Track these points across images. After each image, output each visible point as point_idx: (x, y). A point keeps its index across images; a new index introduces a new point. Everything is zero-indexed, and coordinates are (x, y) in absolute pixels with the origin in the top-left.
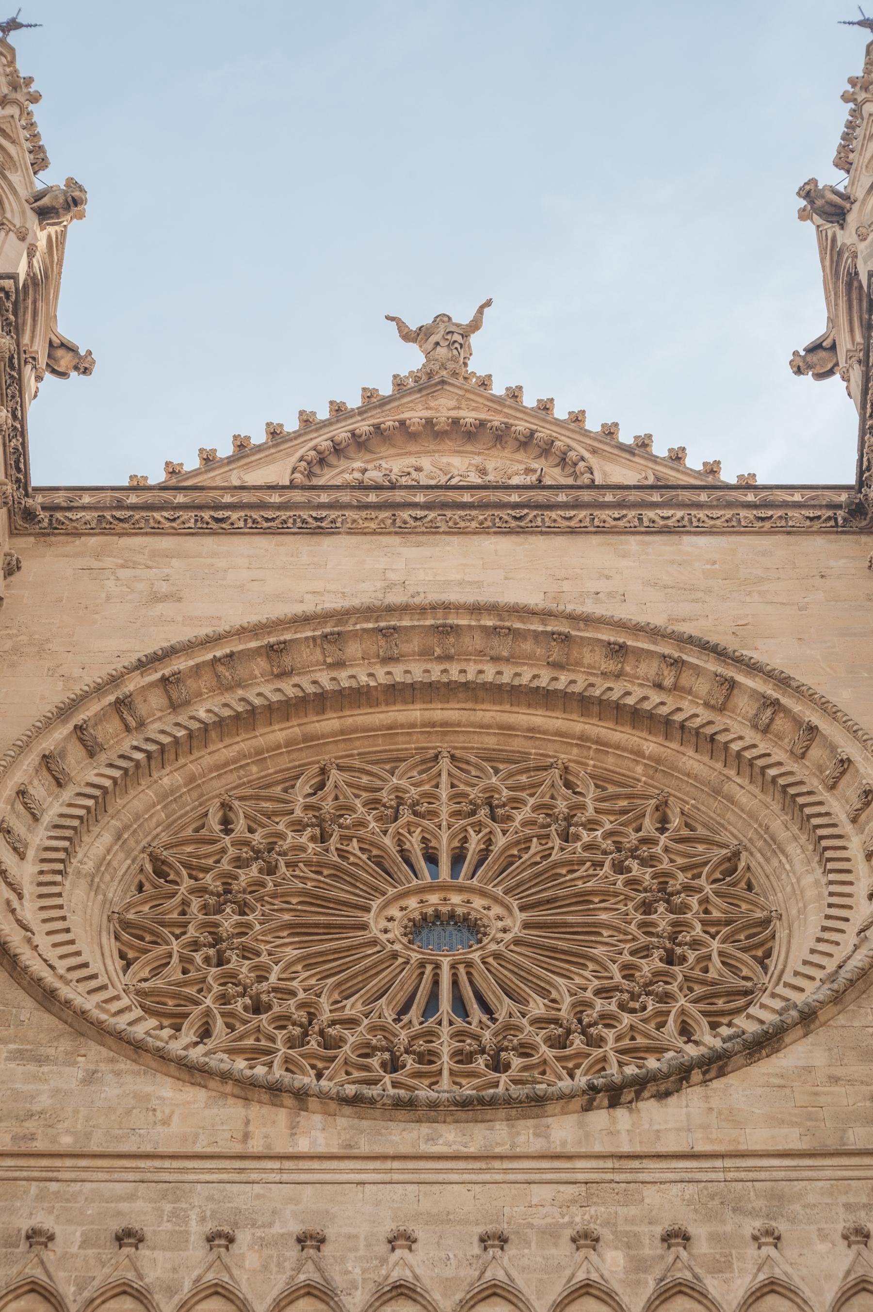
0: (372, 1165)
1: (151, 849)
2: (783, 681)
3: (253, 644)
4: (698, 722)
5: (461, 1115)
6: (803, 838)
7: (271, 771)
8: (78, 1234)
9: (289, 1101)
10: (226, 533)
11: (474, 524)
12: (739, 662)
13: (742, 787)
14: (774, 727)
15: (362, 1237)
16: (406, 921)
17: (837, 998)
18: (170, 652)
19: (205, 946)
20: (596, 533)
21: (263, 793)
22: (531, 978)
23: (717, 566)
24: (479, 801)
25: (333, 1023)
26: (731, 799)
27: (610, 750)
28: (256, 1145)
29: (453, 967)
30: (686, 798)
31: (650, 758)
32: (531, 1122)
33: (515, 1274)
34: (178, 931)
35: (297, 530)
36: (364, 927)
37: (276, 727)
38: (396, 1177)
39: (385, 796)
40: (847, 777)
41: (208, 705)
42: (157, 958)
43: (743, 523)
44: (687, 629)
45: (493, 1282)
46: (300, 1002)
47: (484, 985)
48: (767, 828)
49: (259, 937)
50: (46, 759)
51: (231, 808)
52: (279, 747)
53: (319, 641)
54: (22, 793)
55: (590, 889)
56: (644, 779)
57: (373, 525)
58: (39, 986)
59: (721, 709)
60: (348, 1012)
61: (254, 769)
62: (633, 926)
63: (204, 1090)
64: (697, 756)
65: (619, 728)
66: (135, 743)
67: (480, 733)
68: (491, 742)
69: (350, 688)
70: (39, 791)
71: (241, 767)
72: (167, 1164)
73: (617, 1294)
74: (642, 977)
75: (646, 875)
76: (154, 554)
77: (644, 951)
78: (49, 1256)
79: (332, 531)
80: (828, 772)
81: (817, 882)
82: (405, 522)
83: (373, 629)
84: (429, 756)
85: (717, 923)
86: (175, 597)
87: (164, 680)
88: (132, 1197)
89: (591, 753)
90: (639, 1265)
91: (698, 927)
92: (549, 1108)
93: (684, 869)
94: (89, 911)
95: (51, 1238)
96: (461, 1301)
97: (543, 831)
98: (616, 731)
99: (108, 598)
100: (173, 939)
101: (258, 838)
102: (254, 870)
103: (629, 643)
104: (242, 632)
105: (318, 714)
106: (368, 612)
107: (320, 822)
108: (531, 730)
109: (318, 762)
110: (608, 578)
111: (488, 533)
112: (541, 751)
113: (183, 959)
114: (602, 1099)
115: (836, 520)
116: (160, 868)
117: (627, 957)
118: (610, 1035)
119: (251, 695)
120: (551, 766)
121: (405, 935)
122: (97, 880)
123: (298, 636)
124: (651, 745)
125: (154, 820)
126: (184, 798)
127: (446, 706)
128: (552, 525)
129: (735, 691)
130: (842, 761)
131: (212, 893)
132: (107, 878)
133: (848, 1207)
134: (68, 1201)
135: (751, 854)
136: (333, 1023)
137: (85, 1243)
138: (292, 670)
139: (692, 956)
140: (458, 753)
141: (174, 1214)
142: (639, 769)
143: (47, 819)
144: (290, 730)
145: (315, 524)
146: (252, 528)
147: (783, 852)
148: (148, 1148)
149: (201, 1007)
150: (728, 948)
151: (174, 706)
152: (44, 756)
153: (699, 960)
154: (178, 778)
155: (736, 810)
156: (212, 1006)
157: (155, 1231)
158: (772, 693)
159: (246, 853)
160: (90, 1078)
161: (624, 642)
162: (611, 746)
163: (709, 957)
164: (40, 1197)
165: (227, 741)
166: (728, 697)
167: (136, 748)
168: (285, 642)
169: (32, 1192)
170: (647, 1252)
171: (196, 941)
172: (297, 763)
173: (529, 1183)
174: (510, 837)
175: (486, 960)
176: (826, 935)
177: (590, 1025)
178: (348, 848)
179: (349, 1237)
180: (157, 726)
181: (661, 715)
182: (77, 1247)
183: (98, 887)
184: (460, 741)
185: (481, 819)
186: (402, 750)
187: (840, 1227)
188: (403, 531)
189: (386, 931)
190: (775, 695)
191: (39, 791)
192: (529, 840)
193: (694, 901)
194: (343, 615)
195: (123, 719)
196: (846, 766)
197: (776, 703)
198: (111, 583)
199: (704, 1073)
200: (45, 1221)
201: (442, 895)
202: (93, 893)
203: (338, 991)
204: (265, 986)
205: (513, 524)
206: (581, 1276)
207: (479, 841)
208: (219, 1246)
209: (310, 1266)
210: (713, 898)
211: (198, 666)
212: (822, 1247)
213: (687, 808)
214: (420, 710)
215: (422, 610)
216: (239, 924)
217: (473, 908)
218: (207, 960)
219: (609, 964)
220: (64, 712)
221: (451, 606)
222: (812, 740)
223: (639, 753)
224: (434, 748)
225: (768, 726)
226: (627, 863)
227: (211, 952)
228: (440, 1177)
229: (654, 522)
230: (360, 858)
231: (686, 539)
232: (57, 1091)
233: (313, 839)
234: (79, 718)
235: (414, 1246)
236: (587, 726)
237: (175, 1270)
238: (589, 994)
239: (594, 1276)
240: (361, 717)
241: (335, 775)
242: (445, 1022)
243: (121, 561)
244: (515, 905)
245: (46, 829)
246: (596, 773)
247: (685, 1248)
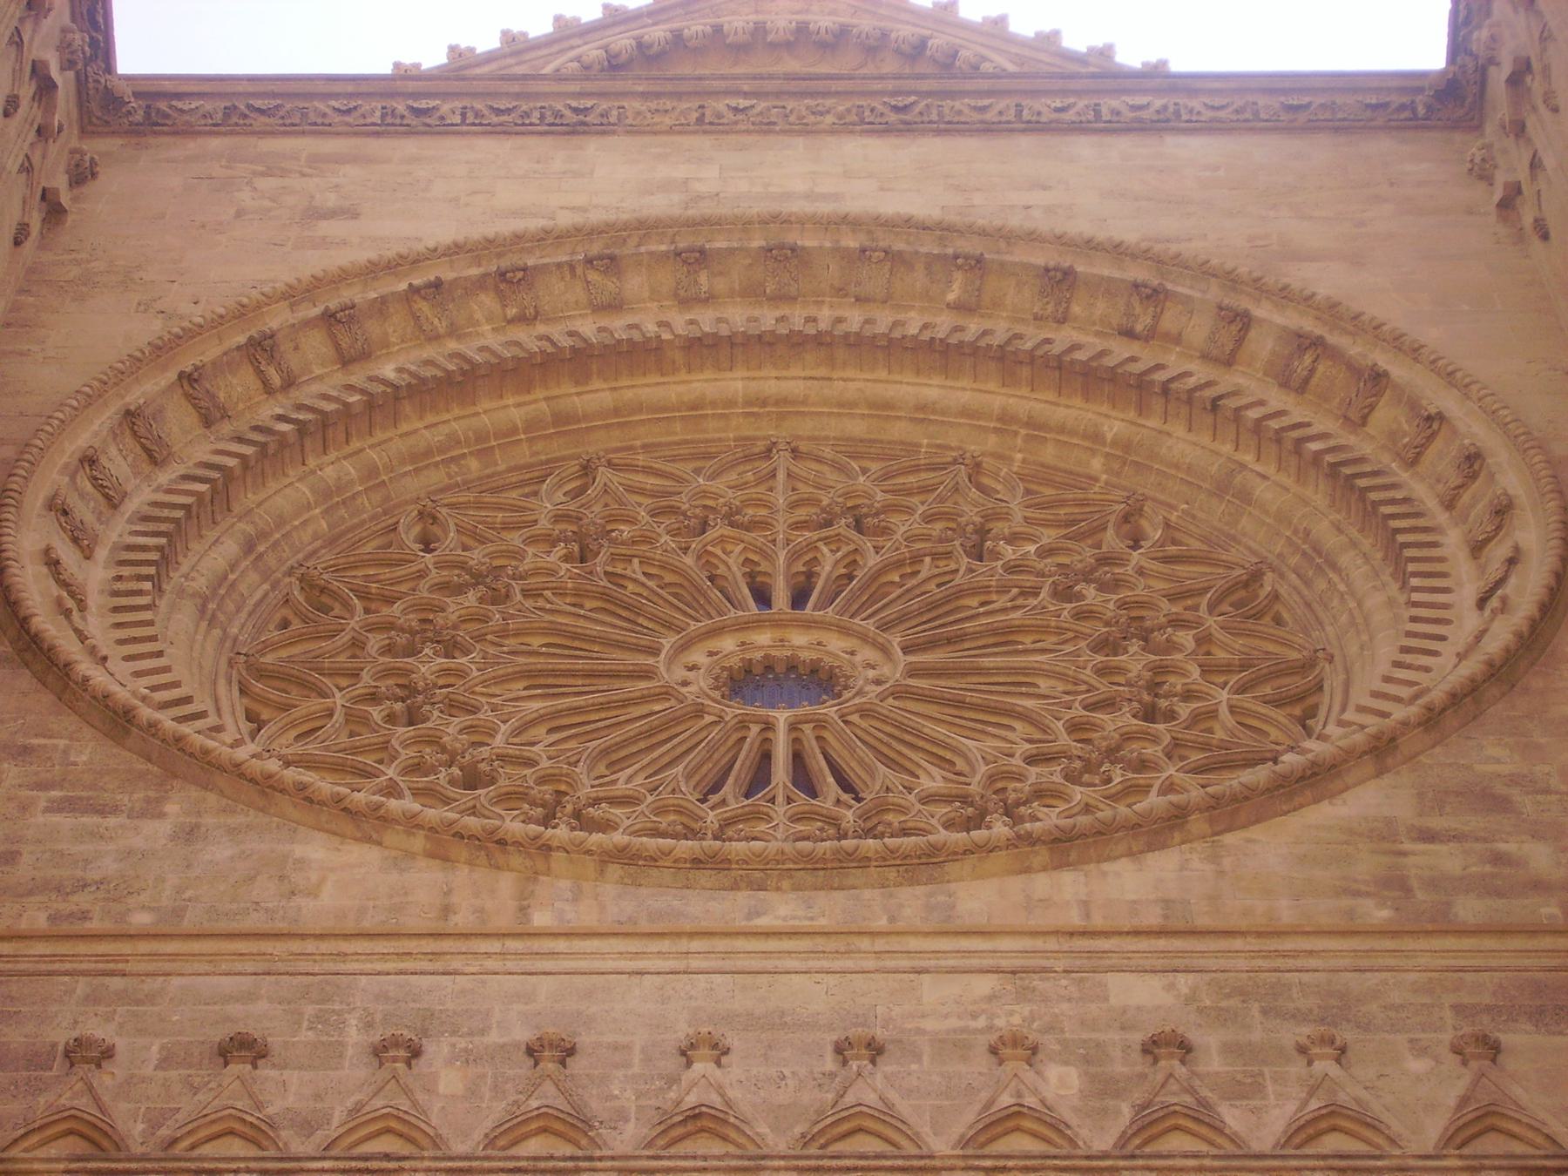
0: (655, 946)
1: (303, 570)
2: (1331, 311)
3: (474, 271)
4: (1191, 382)
5: (808, 878)
6: (1366, 543)
7: (502, 467)
8: (155, 1048)
10: (429, 131)
11: (829, 119)
12: (1258, 287)
13: (1264, 477)
14: (1314, 381)
15: (637, 1049)
16: (717, 670)
17: (1432, 720)
19: (388, 699)
20: (1023, 131)
21: (487, 498)
22: (921, 743)
23: (1221, 173)
24: (838, 510)
25: (596, 802)
26: (1245, 496)
27: (1048, 436)
28: (462, 919)
29: (793, 727)
30: (1174, 502)
31: (1114, 443)
32: (920, 890)
33: (893, 1096)
34: (344, 682)
35: (547, 128)
36: (647, 674)
37: (511, 401)
38: (695, 963)
39: (683, 502)
40: (1438, 444)
41: (402, 360)
42: (309, 718)
43: (1263, 116)
45: (858, 1109)
46: (542, 773)
47: (845, 753)
48: (1307, 533)
49: (477, 689)
50: (130, 415)
51: (434, 518)
52: (514, 430)
53: (579, 271)
54: (89, 460)
55: (1017, 623)
56: (1104, 477)
57: (668, 121)
58: (107, 706)
59: (1229, 362)
60: (621, 788)
61: (474, 464)
62: (1088, 671)
63: (375, 849)
64: (1192, 437)
65: (1063, 401)
66: (279, 411)
67: (839, 415)
69: (630, 340)
70: (118, 463)
71: (452, 459)
72: (310, 946)
73: (1068, 1127)
74: (1104, 738)
75: (1107, 604)
76: (315, 160)
77: (1108, 704)
78: (105, 1081)
79: (604, 128)
80: (1406, 440)
81: (1391, 602)
82: (719, 116)
83: (666, 255)
84: (756, 450)
85: (1227, 669)
87: (329, 317)
88: (250, 997)
89: (1019, 441)
90: (1103, 1088)
91: (1196, 672)
92: (952, 868)
93: (1173, 598)
94: (197, 646)
95: (108, 1053)
96: (803, 1136)
97: (941, 548)
98: (1058, 405)
99: (239, 214)
100: (335, 690)
101: (477, 556)
102: (471, 598)
103: (1080, 269)
104: (455, 250)
105: (577, 383)
107: (579, 537)
108: (921, 408)
109: (579, 457)
110: (1045, 188)
111: (851, 132)
112: (938, 442)
113: (350, 716)
115: (1414, 110)
116: (319, 594)
117: (1078, 711)
119: (469, 348)
120: (955, 462)
121: (716, 688)
122: (212, 606)
123: (546, 260)
124: (1115, 424)
125: (310, 530)
126: (359, 501)
127: (785, 373)
128: (956, 119)
129: (1252, 334)
130: (1429, 418)
131: (403, 630)
132: (230, 606)
133: (1458, 1009)
134: (138, 1002)
135: (1282, 576)
136: (596, 802)
137: (165, 1062)
138: (537, 313)
139: (1184, 710)
140: (803, 447)
141: (319, 1017)
142: (1096, 464)
143: (132, 506)
144: (533, 406)
145: (576, 118)
146: (474, 124)
147: (1334, 566)
148: (281, 926)
149: (378, 780)
150: (1246, 701)
152: (128, 413)
153: (1196, 718)
154: (350, 469)
155: (1256, 512)
156: (398, 779)
157: (286, 1043)
159: (455, 576)
160: (189, 834)
161: (1071, 267)
162: (1050, 430)
163: (1212, 714)
164: (92, 999)
165: (430, 418)
166: (1240, 342)
167: (281, 418)
168: (525, 269)
169: (79, 991)
170: (1119, 1068)
171: (374, 694)
172: (543, 458)
173: (919, 973)
174: (887, 555)
175: (850, 718)
176: (1408, 658)
177: (1018, 804)
178: (628, 572)
179: (616, 1047)
180: (315, 388)
181: (1130, 374)
182: (152, 1067)
183: (214, 616)
184: (806, 427)
185: (841, 530)
186: (713, 441)
187: (1447, 1037)
189: (685, 683)
190: (1318, 331)
191: (118, 463)
192: (916, 559)
193: (1186, 638)
195: (260, 373)
196: (1435, 426)
197: (1317, 343)
198: (245, 197)
199: (1211, 821)
201: (778, 634)
202: (204, 624)
203: (605, 762)
204: (485, 752)
205: (893, 117)
206: (1006, 1100)
207: (837, 562)
208: (395, 1060)
209: (548, 1087)
210: (1219, 635)
211: (383, 300)
212: (1418, 1065)
213: (1173, 517)
214: (742, 379)
215: (745, 224)
216: (446, 672)
217: (827, 652)
218: (391, 718)
219: (1048, 720)
220: (161, 350)
221: (793, 219)
222: (1379, 395)
223: (1096, 437)
224: (765, 438)
225: (1306, 381)
226: (1078, 588)
227: (398, 706)
228: (769, 964)
229: (1118, 113)
230: (643, 585)
231: (1170, 140)
232: (130, 852)
233: (567, 558)
235: (724, 1060)
236: (1011, 401)
237: (318, 1097)
238: (1017, 761)
239: (1030, 1101)
240: (647, 390)
241: (604, 475)
242: (780, 799)
243: (260, 168)
244: (895, 640)
245: (130, 521)
246: (1027, 471)
247: (1183, 1062)
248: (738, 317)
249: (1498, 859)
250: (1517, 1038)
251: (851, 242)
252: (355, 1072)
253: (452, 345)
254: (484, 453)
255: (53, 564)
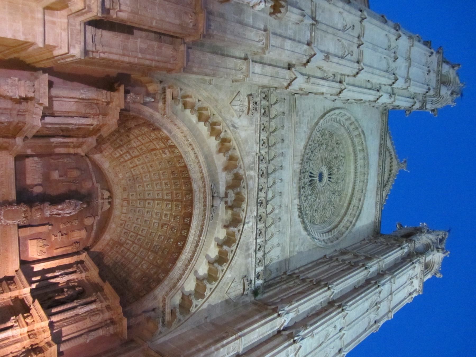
3: (364, 147)
9: (301, 162)
18: (364, 135)
26: (337, 217)
44: (362, 211)
54: (345, 115)
68: (347, 181)
86: (371, 133)
87: (360, 134)
88: (288, 140)
90: (276, 215)
104: (366, 145)
106: (368, 164)
114: (299, 207)
118: (306, 203)
124: (346, 205)
133: (282, 243)
137: (282, 135)
142: (342, 203)
143: (341, 118)
151: (356, 135)
158: (353, 223)
160: (305, 132)
188: (379, 166)
191: (345, 117)
194: (368, 159)
200: (285, 128)
212: (277, 240)
220: (356, 120)
223: (344, 203)
234: (355, 122)
248: (359, 170)
249: (297, 245)
250: (279, 249)
251: (365, 181)
252: (281, 151)
253: (357, 145)
254: (346, 148)
255: (334, 114)
